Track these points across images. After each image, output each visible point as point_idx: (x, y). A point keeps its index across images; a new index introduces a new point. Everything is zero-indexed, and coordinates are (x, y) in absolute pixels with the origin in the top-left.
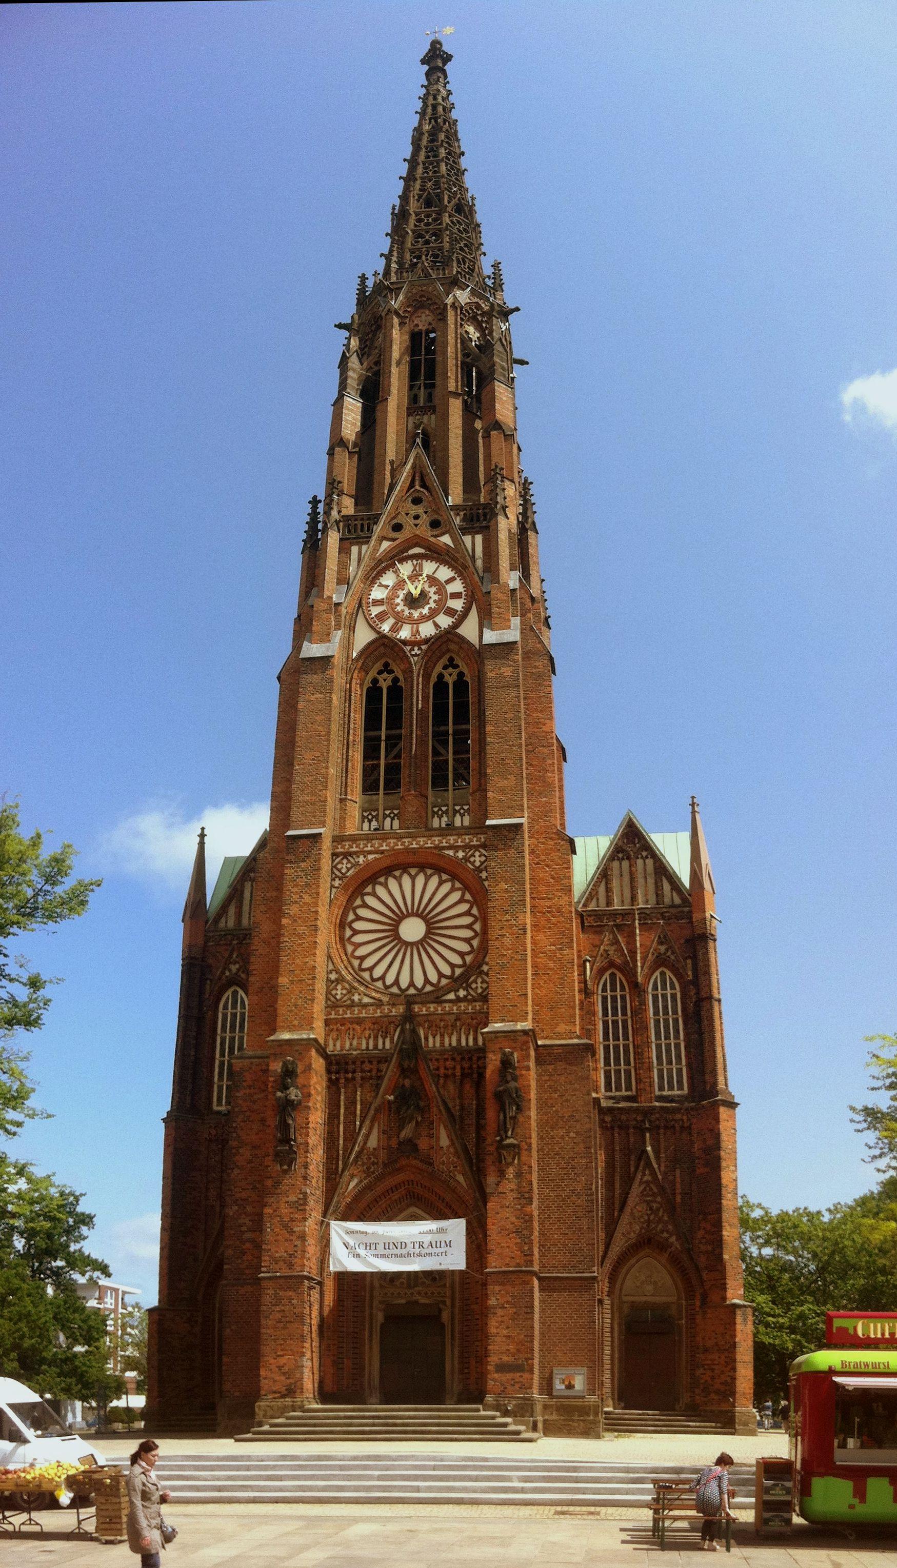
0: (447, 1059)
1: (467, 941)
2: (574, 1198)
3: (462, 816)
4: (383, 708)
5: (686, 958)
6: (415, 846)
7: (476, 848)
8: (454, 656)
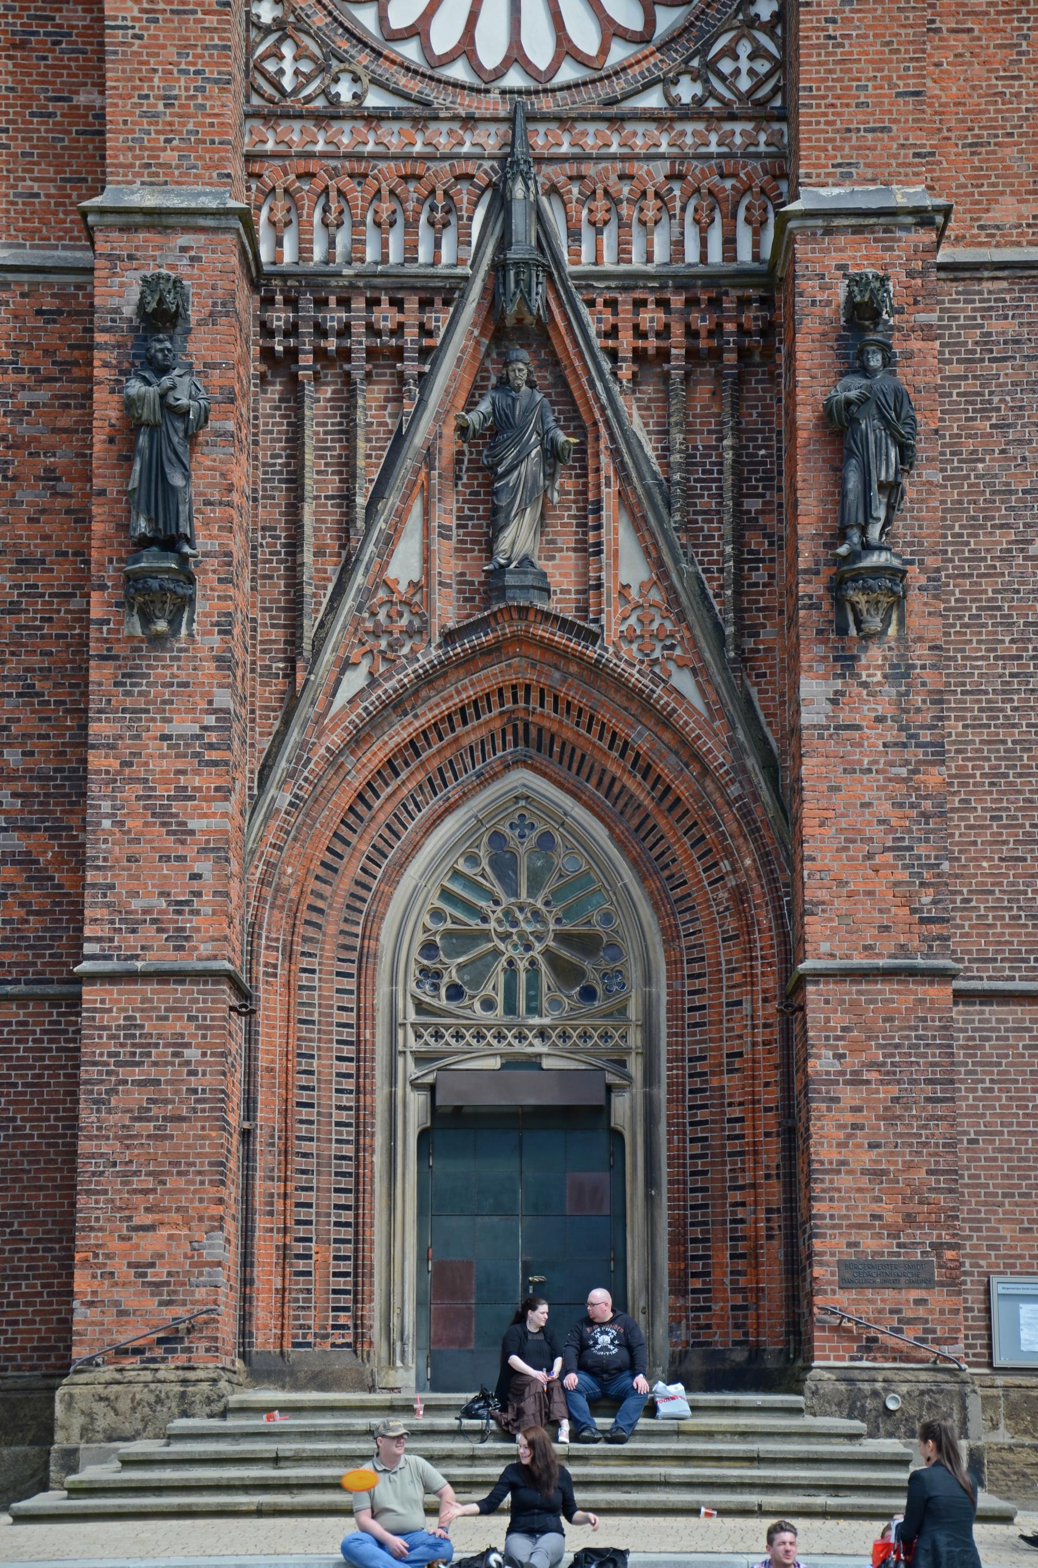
0: (640, 304)
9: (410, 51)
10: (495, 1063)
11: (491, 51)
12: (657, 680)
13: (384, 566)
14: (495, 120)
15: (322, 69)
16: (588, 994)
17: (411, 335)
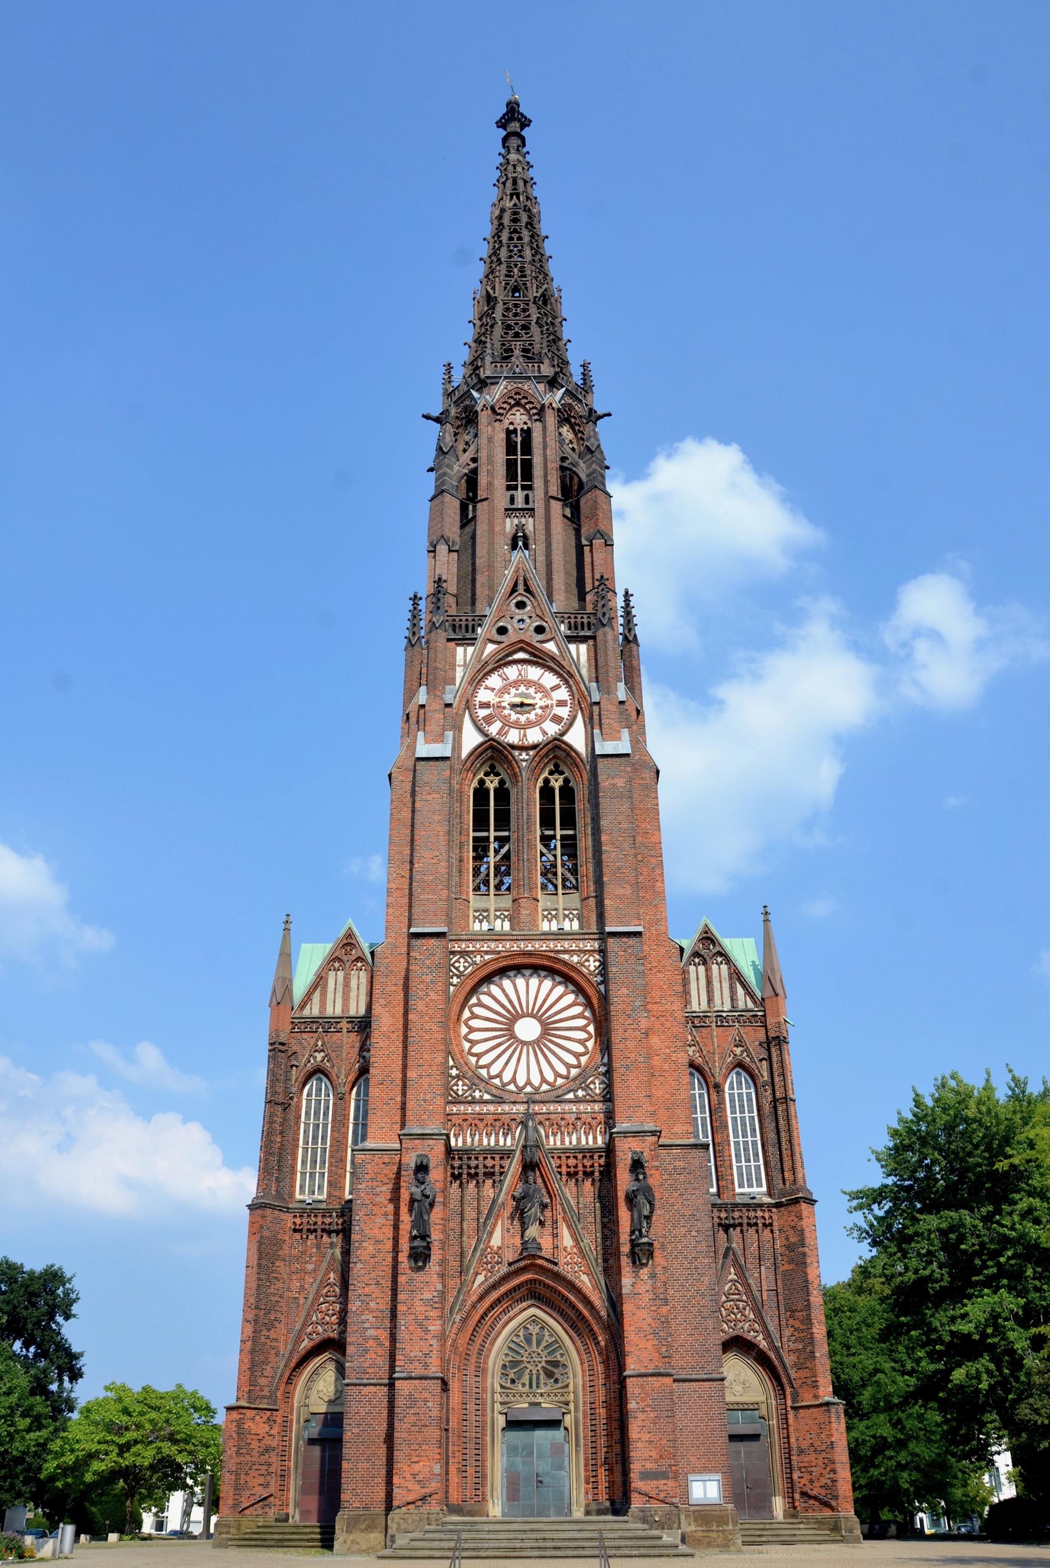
2: (699, 1298)
3: (571, 920)
4: (492, 809)
5: (761, 1060)
6: (529, 948)
8: (560, 763)
9: (497, 1081)
10: (526, 1405)
11: (521, 1082)
12: (576, 1278)
13: (489, 1241)
15: (470, 1088)
16: (556, 1381)
17: (497, 1168)
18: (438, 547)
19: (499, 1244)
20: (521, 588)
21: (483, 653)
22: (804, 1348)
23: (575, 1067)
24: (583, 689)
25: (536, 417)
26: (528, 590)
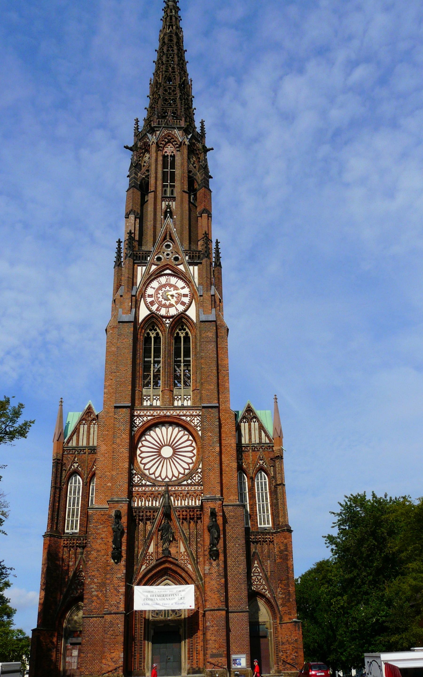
0: (183, 511)
1: (191, 458)
2: (239, 575)
6: (168, 414)
7: (195, 416)
12: (185, 566)
14: (164, 486)
18: (130, 216)
19: (152, 551)
20: (168, 237)
21: (150, 270)
22: (285, 597)
23: (187, 469)
24: (196, 288)
25: (178, 149)
26: (171, 239)
